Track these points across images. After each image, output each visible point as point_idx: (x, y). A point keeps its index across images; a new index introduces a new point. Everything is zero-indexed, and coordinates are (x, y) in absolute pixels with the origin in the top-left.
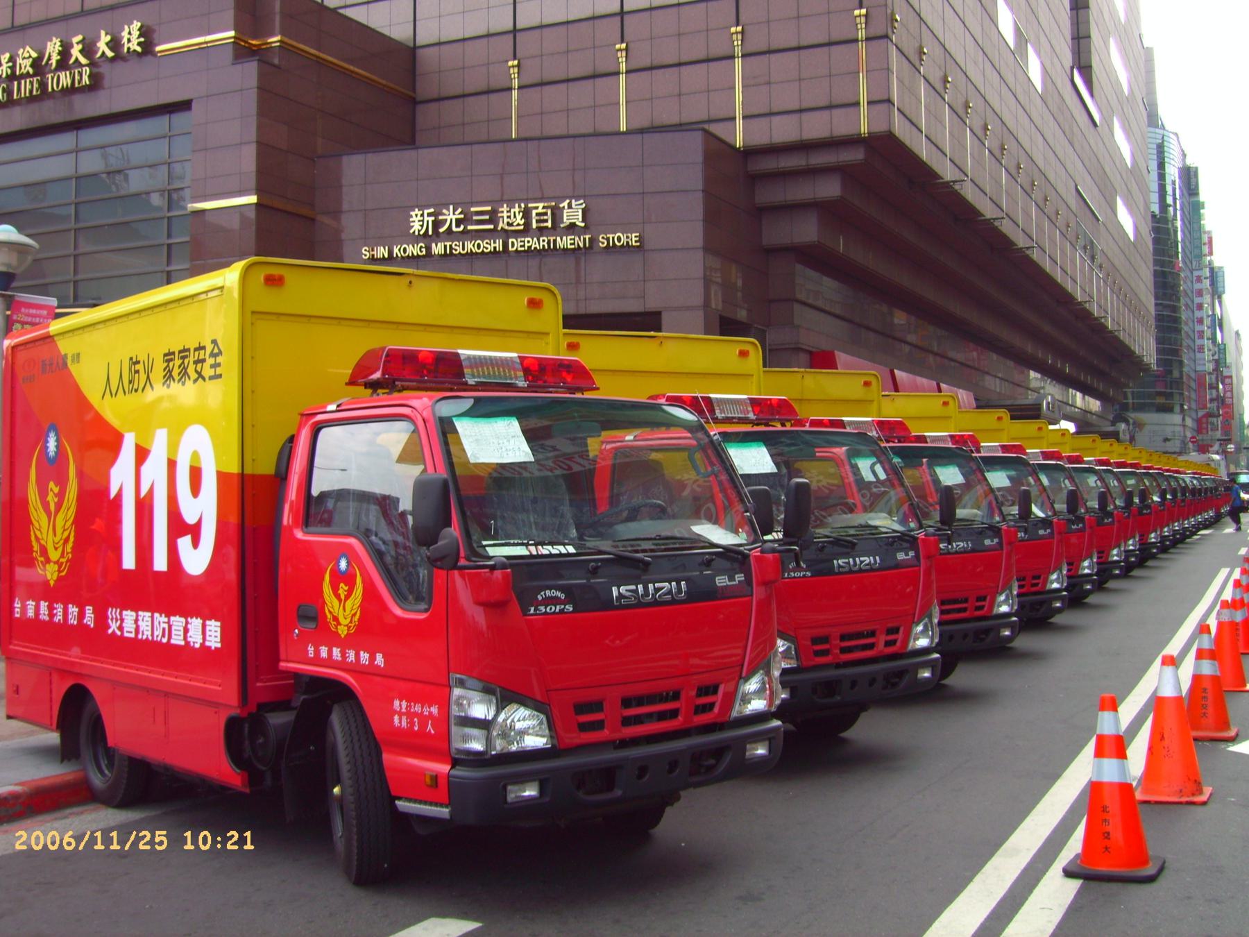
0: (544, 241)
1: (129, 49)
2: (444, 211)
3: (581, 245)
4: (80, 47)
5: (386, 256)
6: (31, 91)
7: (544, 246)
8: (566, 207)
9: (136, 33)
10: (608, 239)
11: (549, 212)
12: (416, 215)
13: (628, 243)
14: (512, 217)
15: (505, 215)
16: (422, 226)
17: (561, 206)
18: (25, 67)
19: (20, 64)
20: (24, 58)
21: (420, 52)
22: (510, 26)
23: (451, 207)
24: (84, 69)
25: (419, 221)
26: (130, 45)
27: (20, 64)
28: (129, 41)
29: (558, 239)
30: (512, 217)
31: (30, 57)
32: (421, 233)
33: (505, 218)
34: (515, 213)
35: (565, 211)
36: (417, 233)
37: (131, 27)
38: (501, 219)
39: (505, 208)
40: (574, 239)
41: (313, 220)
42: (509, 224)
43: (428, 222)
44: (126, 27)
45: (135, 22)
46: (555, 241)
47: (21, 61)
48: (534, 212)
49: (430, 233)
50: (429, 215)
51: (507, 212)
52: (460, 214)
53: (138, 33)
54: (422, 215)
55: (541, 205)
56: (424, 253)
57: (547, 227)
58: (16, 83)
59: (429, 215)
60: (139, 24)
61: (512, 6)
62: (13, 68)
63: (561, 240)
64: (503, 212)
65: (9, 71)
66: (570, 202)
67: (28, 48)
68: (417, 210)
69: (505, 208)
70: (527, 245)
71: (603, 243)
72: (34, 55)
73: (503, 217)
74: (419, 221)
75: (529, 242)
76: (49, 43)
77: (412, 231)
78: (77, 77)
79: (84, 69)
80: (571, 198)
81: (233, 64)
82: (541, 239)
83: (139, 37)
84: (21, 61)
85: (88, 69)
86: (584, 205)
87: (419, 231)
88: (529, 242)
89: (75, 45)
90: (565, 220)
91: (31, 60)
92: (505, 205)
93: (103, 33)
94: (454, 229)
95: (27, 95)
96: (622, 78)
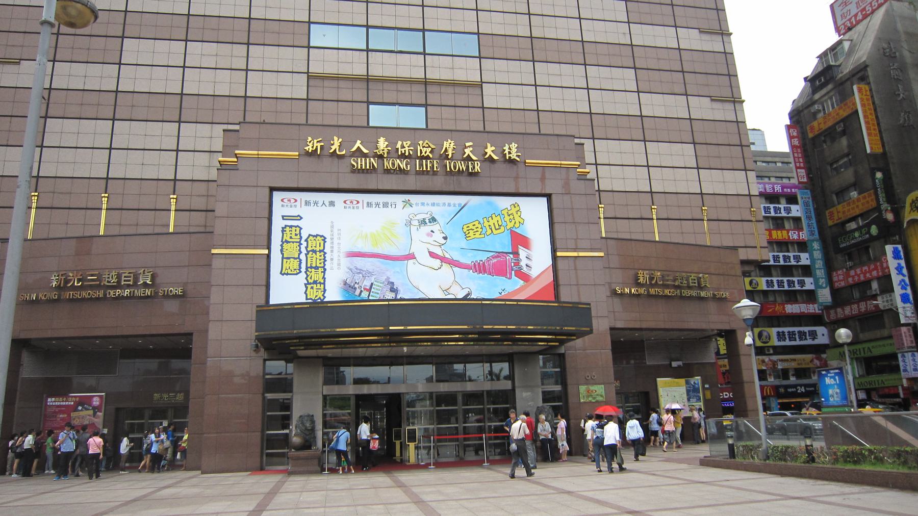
1: (510, 157)
9: (514, 150)
18: (426, 152)
19: (421, 150)
20: (423, 147)
24: (476, 163)
27: (421, 150)
28: (510, 153)
31: (429, 147)
44: (506, 145)
47: (421, 148)
53: (516, 150)
58: (424, 161)
60: (516, 145)
67: (427, 141)
72: (433, 147)
78: (470, 167)
84: (421, 148)
91: (430, 149)
93: (489, 145)
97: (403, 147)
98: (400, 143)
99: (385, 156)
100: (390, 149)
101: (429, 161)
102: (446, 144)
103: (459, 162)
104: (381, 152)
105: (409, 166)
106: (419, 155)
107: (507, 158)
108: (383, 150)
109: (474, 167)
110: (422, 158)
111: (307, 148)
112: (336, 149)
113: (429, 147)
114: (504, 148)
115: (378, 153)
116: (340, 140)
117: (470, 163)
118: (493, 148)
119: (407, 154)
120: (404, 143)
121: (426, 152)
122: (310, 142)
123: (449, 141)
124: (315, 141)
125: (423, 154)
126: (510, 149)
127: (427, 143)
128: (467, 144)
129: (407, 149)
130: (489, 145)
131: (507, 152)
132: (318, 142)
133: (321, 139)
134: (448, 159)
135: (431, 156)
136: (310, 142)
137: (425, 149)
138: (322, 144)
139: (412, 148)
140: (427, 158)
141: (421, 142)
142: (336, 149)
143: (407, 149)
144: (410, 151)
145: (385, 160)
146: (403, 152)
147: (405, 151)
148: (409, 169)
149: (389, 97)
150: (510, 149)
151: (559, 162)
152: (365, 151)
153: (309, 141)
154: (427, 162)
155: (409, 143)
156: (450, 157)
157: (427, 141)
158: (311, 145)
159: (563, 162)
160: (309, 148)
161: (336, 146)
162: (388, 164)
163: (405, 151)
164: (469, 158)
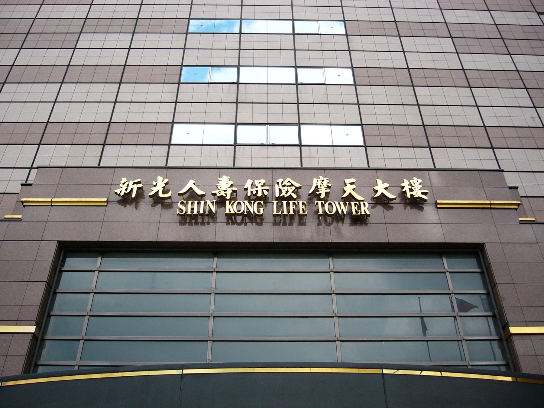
18: (287, 192)
19: (280, 190)
20: (284, 186)
24: (362, 203)
31: (292, 185)
47: (281, 187)
53: (421, 186)
60: (420, 181)
67: (288, 179)
72: (298, 185)
76: (315, 180)
78: (354, 208)
84: (281, 187)
89: (348, 185)
91: (293, 188)
93: (379, 181)
98: (250, 182)
99: (228, 197)
100: (235, 189)
101: (291, 203)
102: (316, 182)
103: (337, 203)
104: (223, 193)
105: (262, 209)
106: (277, 195)
107: (409, 196)
108: (225, 191)
110: (282, 198)
112: (158, 192)
113: (292, 185)
114: (403, 185)
115: (218, 195)
116: (166, 180)
117: (353, 203)
118: (386, 185)
119: (260, 194)
121: (287, 192)
122: (124, 184)
123: (321, 178)
124: (131, 182)
125: (284, 193)
127: (289, 182)
128: (347, 181)
129: (260, 189)
130: (379, 181)
131: (407, 189)
132: (134, 183)
133: (139, 180)
134: (321, 200)
135: (295, 196)
136: (124, 184)
137: (286, 188)
138: (140, 185)
139: (267, 188)
140: (290, 198)
141: (280, 181)
142: (158, 192)
143: (260, 189)
144: (264, 191)
145: (227, 202)
146: (254, 192)
147: (257, 191)
148: (262, 212)
150: (411, 185)
152: (199, 192)
153: (123, 182)
154: (288, 204)
156: (322, 196)
157: (288, 179)
158: (125, 187)
160: (122, 190)
161: (160, 187)
162: (231, 208)
163: (257, 191)
164: (351, 198)
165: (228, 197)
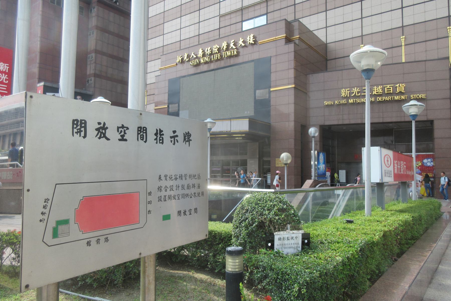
0: (390, 98)
1: (250, 43)
2: (353, 89)
3: (404, 98)
4: (233, 43)
5: (333, 104)
6: (217, 58)
7: (390, 99)
8: (398, 86)
9: (252, 38)
10: (414, 96)
11: (391, 88)
12: (343, 91)
13: (422, 97)
14: (378, 90)
15: (375, 90)
16: (345, 94)
17: (396, 86)
20: (215, 48)
21: (328, 45)
22: (361, 35)
23: (356, 88)
24: (235, 50)
25: (344, 93)
26: (250, 41)
28: (250, 40)
29: (395, 97)
30: (378, 90)
31: (217, 47)
32: (345, 96)
33: (375, 90)
34: (379, 89)
35: (397, 88)
36: (343, 96)
37: (250, 36)
38: (374, 91)
39: (375, 87)
40: (401, 97)
41: (306, 93)
42: (377, 92)
43: (347, 93)
45: (252, 34)
46: (394, 98)
48: (386, 88)
49: (348, 96)
50: (348, 91)
51: (376, 89)
52: (358, 90)
54: (345, 91)
55: (388, 86)
56: (346, 103)
57: (390, 93)
59: (348, 91)
60: (253, 35)
61: (363, 26)
62: (212, 51)
63: (396, 97)
64: (374, 89)
65: (210, 53)
66: (400, 85)
67: (216, 45)
68: (343, 89)
69: (375, 87)
70: (383, 99)
71: (412, 98)
72: (218, 47)
73: (374, 90)
74: (344, 93)
75: (384, 98)
76: (223, 43)
77: (342, 96)
78: (232, 53)
79: (235, 50)
80: (399, 83)
81: (285, 45)
82: (389, 97)
83: (253, 39)
84: (214, 49)
85: (236, 50)
86: (405, 86)
87: (344, 96)
88: (384, 98)
89: (232, 43)
90: (397, 91)
91: (217, 48)
92: (375, 87)
93: (241, 39)
94: (357, 95)
95: (216, 59)
96: (403, 47)
97: (207, 50)
98: (207, 49)
109: (234, 52)
111: (177, 61)
120: (208, 49)
126: (250, 38)
149: (251, 15)
150: (250, 38)
151: (274, 38)
155: (210, 48)
159: (277, 37)
165: (201, 57)
